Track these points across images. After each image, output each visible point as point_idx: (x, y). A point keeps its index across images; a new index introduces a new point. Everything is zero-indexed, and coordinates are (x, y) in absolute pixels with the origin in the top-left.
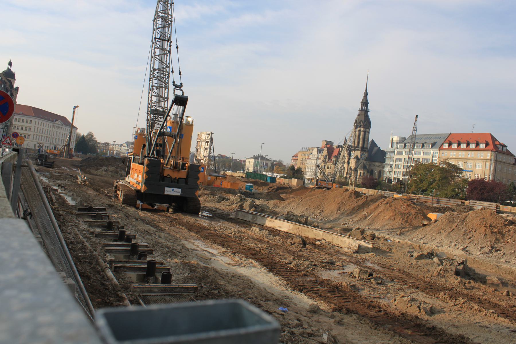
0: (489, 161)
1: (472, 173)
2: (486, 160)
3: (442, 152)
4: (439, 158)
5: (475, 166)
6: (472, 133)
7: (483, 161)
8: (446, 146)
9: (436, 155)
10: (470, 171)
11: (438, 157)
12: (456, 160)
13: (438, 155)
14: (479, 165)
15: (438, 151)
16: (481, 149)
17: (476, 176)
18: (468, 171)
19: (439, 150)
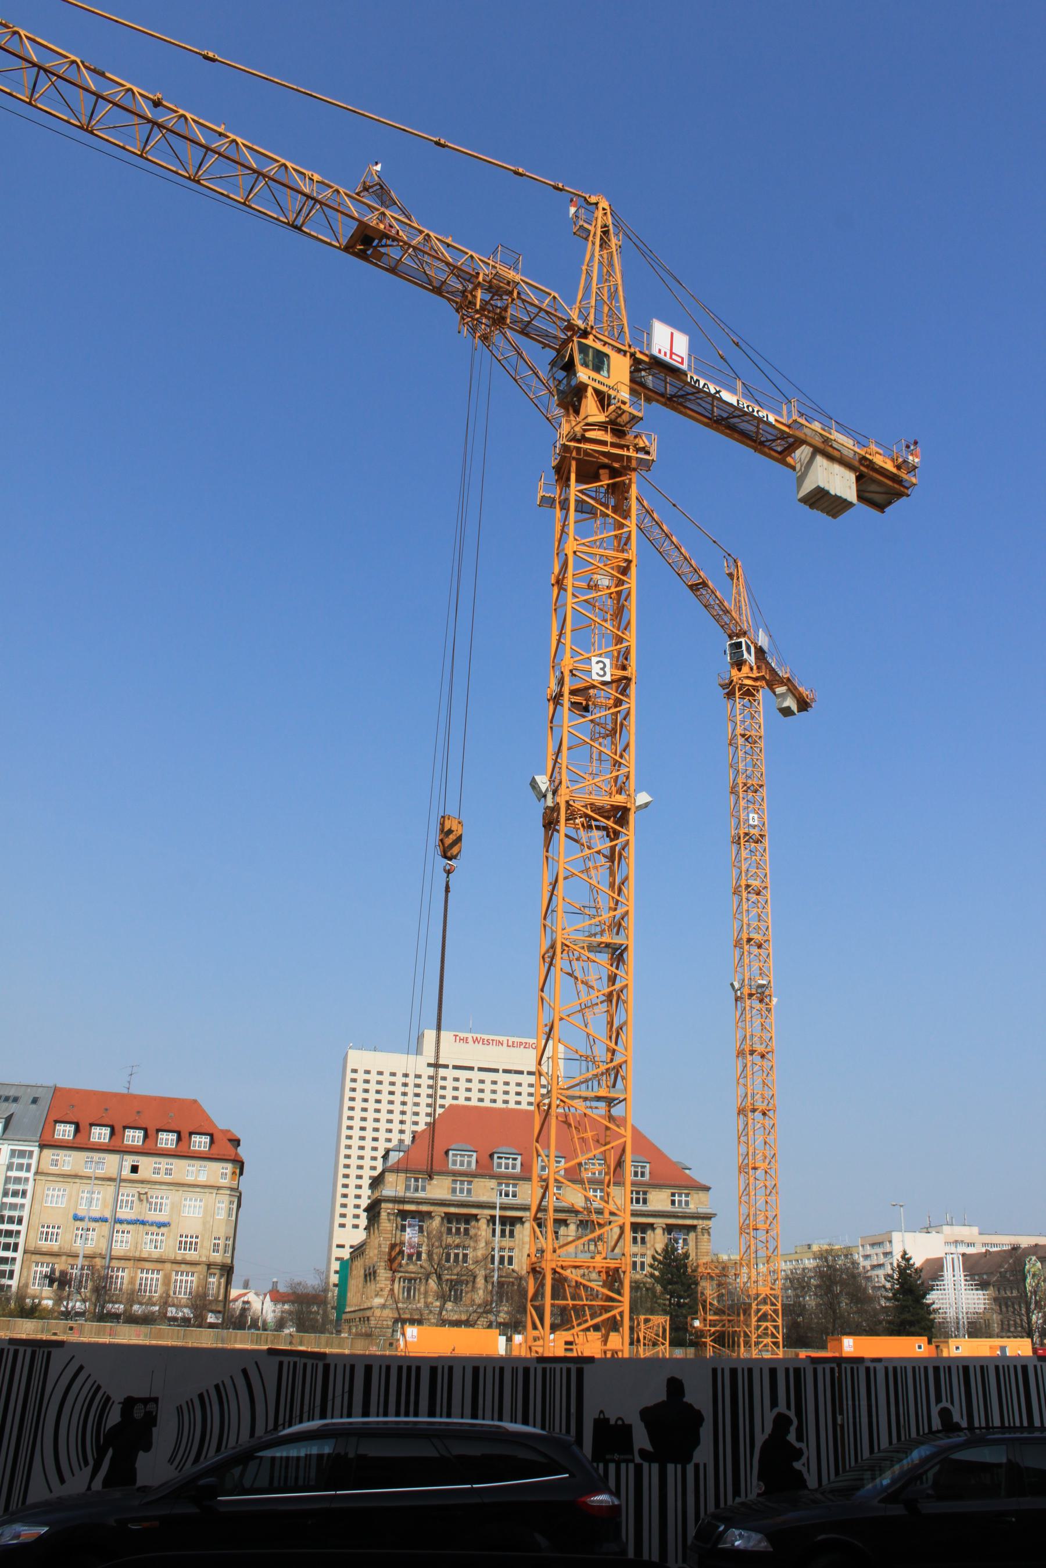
0: (228, 1192)
1: (169, 1231)
2: (219, 1188)
3: (47, 1153)
4: (37, 1173)
5: (176, 1208)
6: (125, 1091)
7: (206, 1190)
8: (65, 1132)
9: (25, 1161)
10: (161, 1225)
11: (33, 1169)
12: (109, 1183)
13: (34, 1162)
14: (198, 1203)
15: (36, 1150)
16: (62, 1140)
17: (189, 1240)
18: (152, 1224)
19: (42, 1146)
